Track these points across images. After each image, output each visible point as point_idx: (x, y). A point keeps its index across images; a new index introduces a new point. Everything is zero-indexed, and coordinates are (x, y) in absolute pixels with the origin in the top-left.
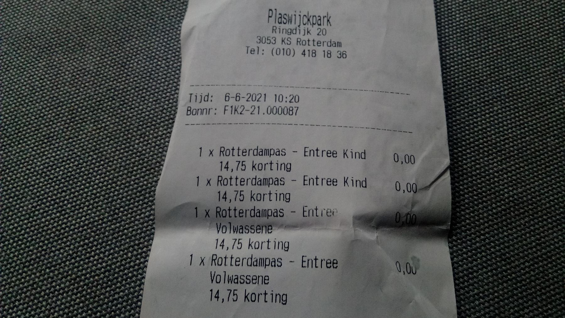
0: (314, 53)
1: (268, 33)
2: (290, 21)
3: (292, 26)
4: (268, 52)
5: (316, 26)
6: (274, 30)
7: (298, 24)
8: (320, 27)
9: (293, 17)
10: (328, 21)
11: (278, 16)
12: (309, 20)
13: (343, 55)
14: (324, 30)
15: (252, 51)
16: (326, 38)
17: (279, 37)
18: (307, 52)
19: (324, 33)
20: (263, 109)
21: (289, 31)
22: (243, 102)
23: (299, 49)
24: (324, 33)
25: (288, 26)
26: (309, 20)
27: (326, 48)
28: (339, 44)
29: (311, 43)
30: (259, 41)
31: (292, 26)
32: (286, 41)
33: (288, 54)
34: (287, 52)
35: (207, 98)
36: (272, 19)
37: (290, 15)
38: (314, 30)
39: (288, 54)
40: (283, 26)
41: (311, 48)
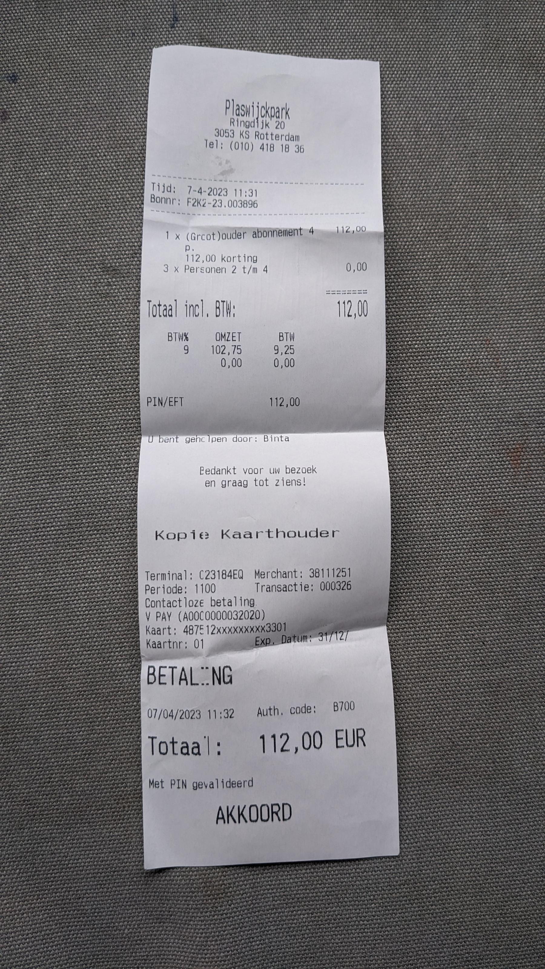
0: (272, 148)
1: (227, 126)
2: (247, 113)
3: (251, 119)
4: (227, 146)
5: (275, 119)
6: (232, 123)
7: (256, 116)
8: (278, 119)
9: (251, 108)
10: (287, 113)
11: (235, 108)
12: (267, 112)
13: (300, 149)
14: (282, 124)
15: (211, 144)
16: (285, 132)
17: (238, 130)
18: (265, 147)
19: (282, 127)
20: (225, 203)
21: (247, 124)
22: (205, 195)
23: (258, 143)
24: (282, 127)
25: (245, 119)
26: (267, 112)
27: (285, 143)
28: (297, 138)
29: (269, 137)
30: (217, 134)
31: (251, 119)
32: (244, 134)
33: (247, 148)
34: (245, 147)
35: (170, 189)
36: (230, 111)
37: (248, 106)
38: (273, 123)
39: (247, 148)
40: (241, 118)
41: (270, 142)
